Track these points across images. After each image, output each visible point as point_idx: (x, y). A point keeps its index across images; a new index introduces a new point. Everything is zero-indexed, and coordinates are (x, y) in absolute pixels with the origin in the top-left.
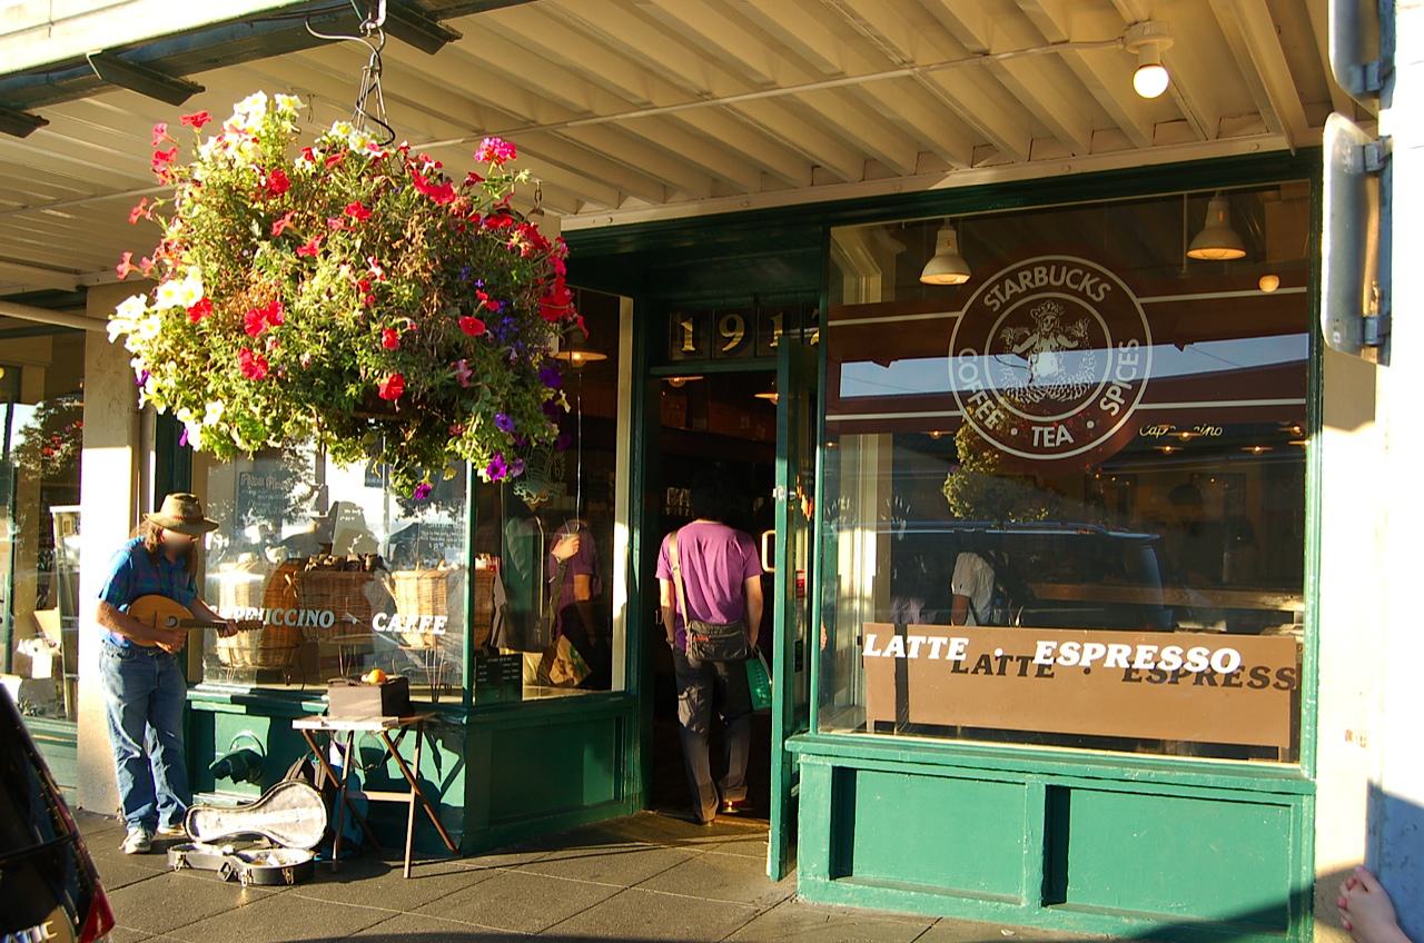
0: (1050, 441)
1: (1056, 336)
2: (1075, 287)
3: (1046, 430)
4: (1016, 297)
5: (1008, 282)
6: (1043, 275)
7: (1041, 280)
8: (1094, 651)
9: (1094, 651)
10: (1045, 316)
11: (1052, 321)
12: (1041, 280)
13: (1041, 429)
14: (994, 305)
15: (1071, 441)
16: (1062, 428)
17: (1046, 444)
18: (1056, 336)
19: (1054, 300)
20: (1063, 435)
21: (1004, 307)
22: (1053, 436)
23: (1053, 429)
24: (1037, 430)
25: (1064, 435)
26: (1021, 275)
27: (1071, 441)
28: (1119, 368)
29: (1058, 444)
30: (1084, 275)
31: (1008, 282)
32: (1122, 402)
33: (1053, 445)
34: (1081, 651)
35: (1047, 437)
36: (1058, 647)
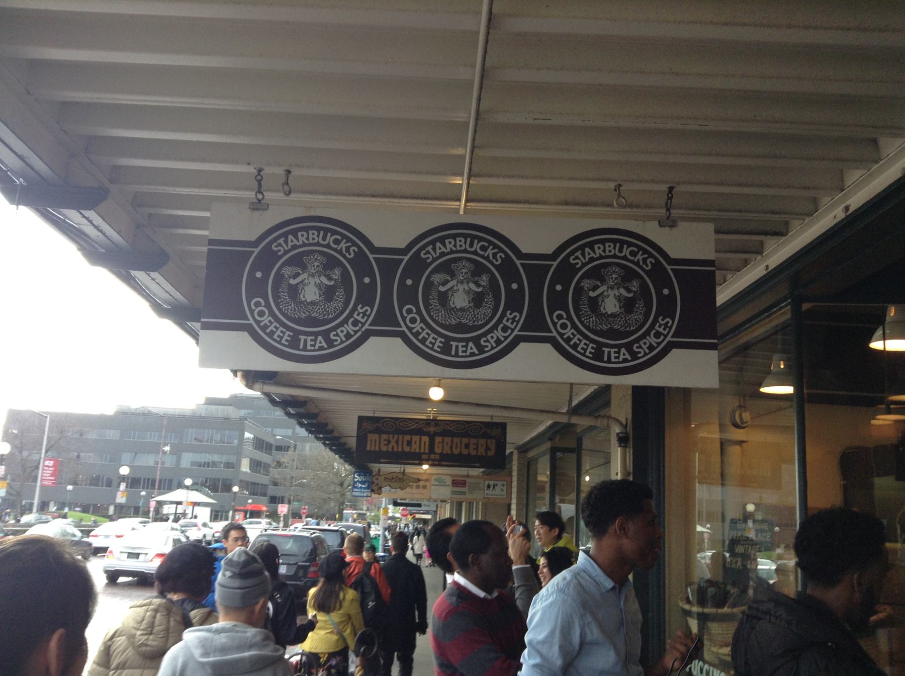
2: (632, 258)
4: (592, 260)
5: (587, 250)
6: (611, 248)
7: (610, 251)
12: (610, 251)
14: (577, 263)
18: (618, 288)
19: (618, 264)
21: (584, 265)
24: (606, 350)
25: (624, 354)
26: (596, 247)
30: (638, 252)
31: (587, 250)
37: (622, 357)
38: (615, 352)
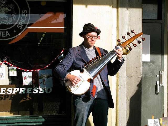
0: (4, 35)
1: (5, 7)
3: (3, 32)
8: (16, 90)
9: (16, 90)
10: (2, 2)
11: (4, 3)
13: (2, 32)
15: (10, 35)
16: (7, 32)
17: (3, 36)
18: (5, 7)
20: (7, 34)
22: (5, 34)
23: (5, 32)
27: (10, 35)
28: (22, 17)
29: (6, 36)
32: (23, 26)
33: (5, 36)
34: (13, 90)
35: (3, 34)
36: (7, 89)
37: (6, 35)
38: (4, 33)
